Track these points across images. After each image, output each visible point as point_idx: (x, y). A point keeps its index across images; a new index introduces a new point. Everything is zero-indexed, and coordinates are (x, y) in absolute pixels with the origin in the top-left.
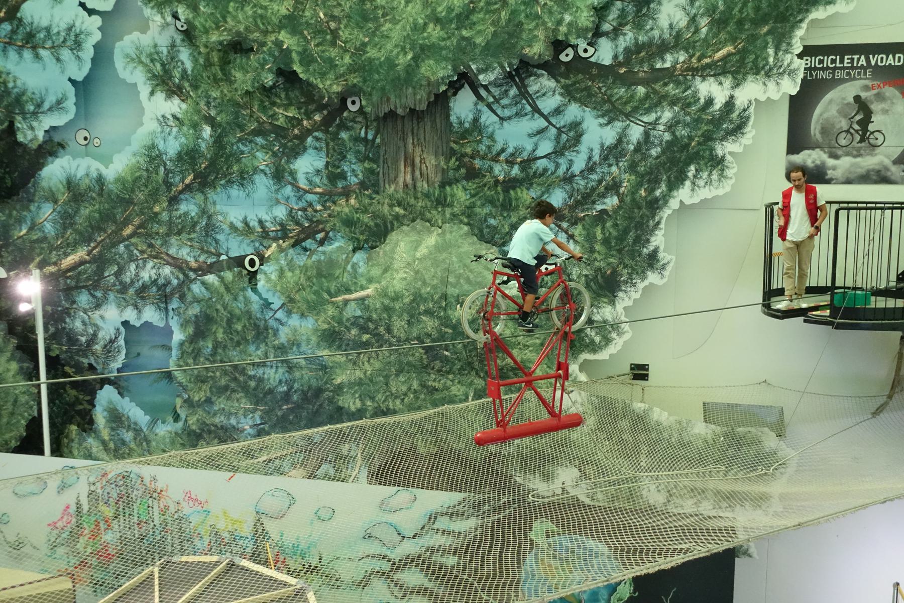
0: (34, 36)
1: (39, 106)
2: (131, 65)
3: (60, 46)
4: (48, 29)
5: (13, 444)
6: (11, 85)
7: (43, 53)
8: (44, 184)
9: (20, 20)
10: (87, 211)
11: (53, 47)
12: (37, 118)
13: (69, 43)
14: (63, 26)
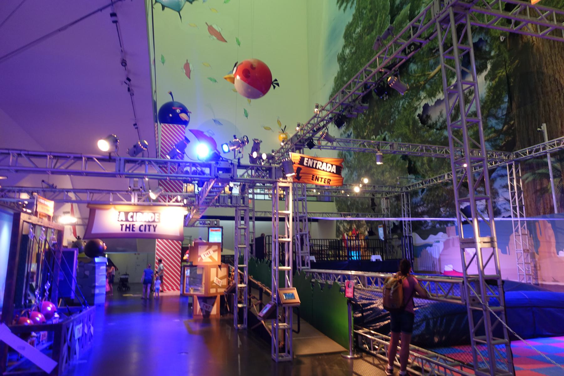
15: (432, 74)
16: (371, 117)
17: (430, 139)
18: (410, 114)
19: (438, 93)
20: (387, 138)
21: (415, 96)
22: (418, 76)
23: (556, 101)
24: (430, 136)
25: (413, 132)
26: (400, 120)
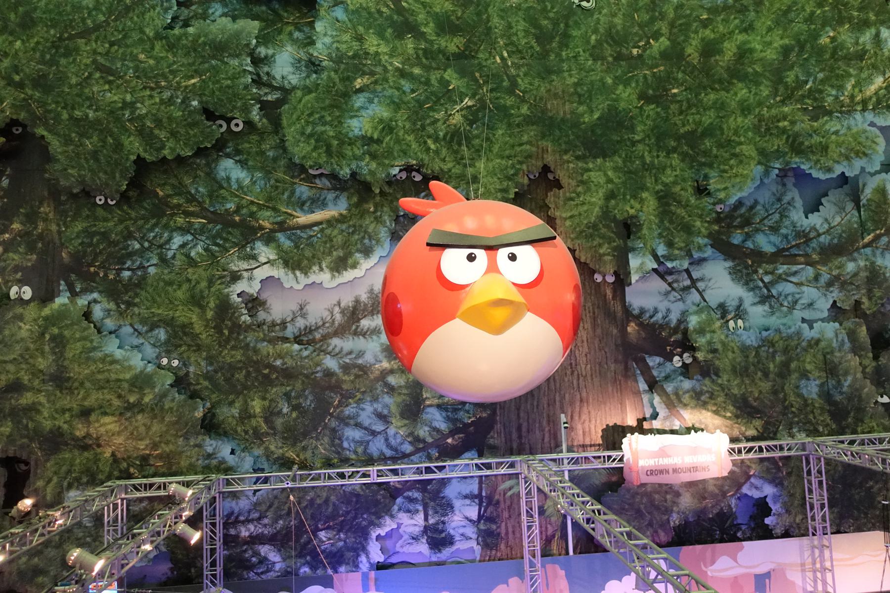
15: (303, 219)
16: (16, 226)
17: (278, 363)
18: (211, 283)
19: (316, 268)
20: (98, 312)
21: (235, 245)
22: (252, 203)
23: (566, 379)
24: (280, 356)
25: (219, 329)
26: (170, 283)
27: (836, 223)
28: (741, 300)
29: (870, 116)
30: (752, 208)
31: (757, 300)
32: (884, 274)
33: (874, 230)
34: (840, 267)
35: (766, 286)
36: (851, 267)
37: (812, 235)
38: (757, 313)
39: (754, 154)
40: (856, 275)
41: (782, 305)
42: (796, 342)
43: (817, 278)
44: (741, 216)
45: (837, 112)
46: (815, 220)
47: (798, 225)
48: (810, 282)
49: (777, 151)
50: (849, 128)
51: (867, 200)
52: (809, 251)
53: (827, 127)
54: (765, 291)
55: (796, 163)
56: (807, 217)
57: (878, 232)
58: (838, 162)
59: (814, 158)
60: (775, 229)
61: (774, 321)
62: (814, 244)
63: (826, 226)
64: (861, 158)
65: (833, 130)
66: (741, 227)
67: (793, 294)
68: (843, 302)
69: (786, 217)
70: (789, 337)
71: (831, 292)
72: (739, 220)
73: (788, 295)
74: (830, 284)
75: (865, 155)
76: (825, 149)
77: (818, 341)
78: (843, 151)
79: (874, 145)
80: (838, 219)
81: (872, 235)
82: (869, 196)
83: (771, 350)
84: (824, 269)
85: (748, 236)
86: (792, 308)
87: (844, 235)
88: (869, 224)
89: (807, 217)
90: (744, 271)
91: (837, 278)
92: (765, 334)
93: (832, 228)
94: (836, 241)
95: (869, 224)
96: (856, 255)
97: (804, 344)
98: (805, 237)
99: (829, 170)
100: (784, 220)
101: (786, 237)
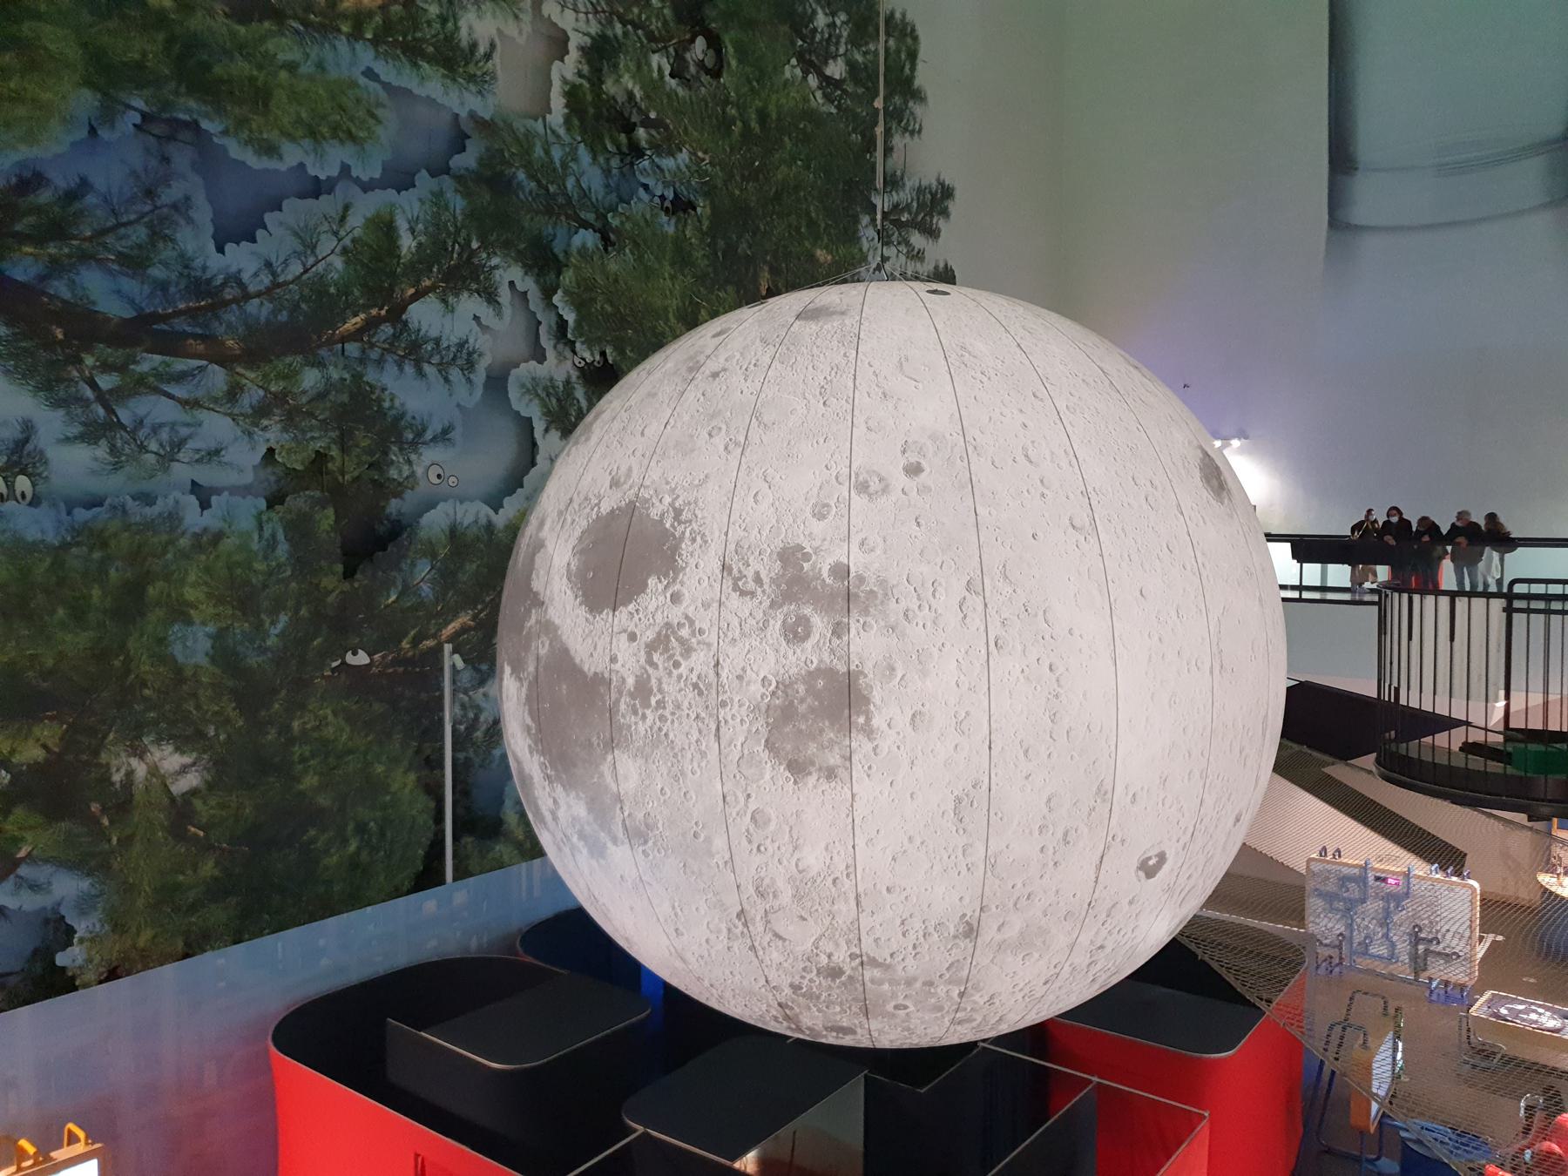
0: (420, 346)
1: (420, 433)
2: (527, 397)
3: (449, 364)
4: (437, 341)
5: (407, 885)
6: (386, 404)
7: (426, 367)
8: (423, 534)
9: (406, 323)
10: (474, 566)
11: (441, 364)
12: (415, 451)
13: (459, 362)
14: (454, 340)
27: (290, 277)
28: (28, 428)
29: (366, 56)
30: (72, 196)
31: (76, 429)
32: (379, 400)
33: (366, 308)
34: (291, 375)
35: (101, 397)
36: (310, 379)
37: (228, 294)
38: (74, 464)
39: (73, 52)
40: (321, 396)
41: (142, 448)
42: (165, 537)
43: (234, 393)
44: (38, 210)
45: (295, 17)
46: (241, 259)
47: (198, 263)
48: (216, 400)
49: (140, 66)
50: (320, 66)
51: (353, 241)
52: (219, 329)
53: (270, 45)
54: (101, 411)
55: (189, 111)
56: (220, 250)
57: (374, 312)
58: (292, 138)
59: (237, 111)
60: (134, 263)
61: (114, 484)
62: (231, 316)
63: (266, 280)
64: (342, 142)
65: (281, 57)
66: (38, 238)
67: (173, 425)
68: (289, 451)
69: (167, 238)
70: (150, 525)
71: (265, 429)
72: (32, 219)
73: (161, 425)
74: (261, 411)
75: (351, 136)
76: (261, 98)
77: (218, 537)
78: (304, 115)
79: (371, 122)
80: (296, 268)
81: (363, 316)
82: (357, 232)
83: (97, 555)
84: (252, 375)
85: (56, 267)
86: (168, 457)
87: (303, 306)
88: (357, 293)
89: (220, 250)
90: (43, 355)
91: (280, 398)
92: (81, 515)
93: (279, 285)
94: (284, 316)
95: (357, 293)
96: (323, 352)
97: (184, 542)
98: (210, 295)
99: (270, 150)
100: (161, 245)
101: (163, 286)
